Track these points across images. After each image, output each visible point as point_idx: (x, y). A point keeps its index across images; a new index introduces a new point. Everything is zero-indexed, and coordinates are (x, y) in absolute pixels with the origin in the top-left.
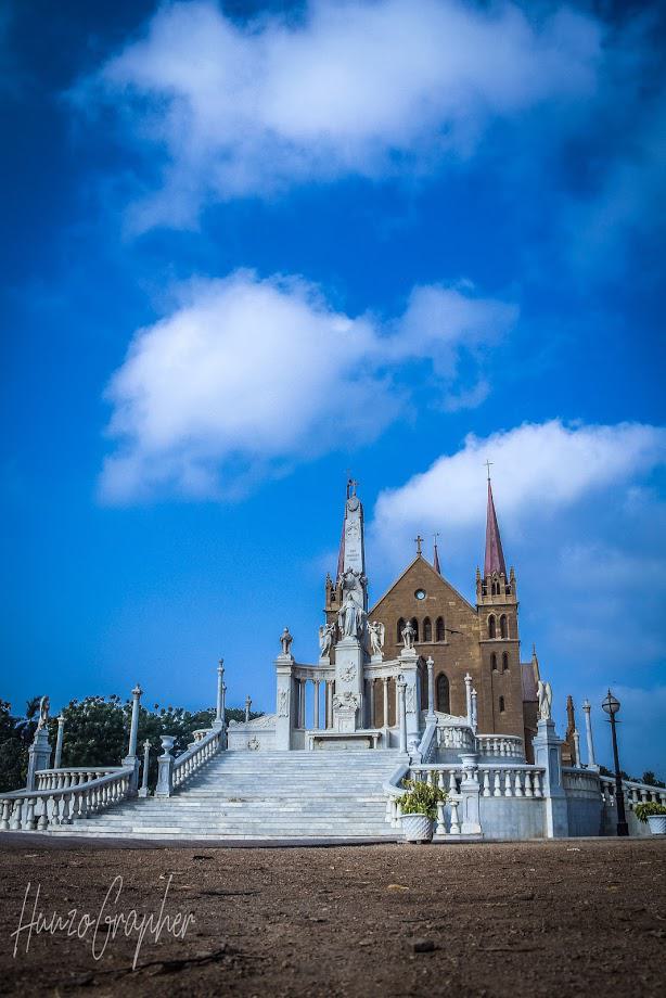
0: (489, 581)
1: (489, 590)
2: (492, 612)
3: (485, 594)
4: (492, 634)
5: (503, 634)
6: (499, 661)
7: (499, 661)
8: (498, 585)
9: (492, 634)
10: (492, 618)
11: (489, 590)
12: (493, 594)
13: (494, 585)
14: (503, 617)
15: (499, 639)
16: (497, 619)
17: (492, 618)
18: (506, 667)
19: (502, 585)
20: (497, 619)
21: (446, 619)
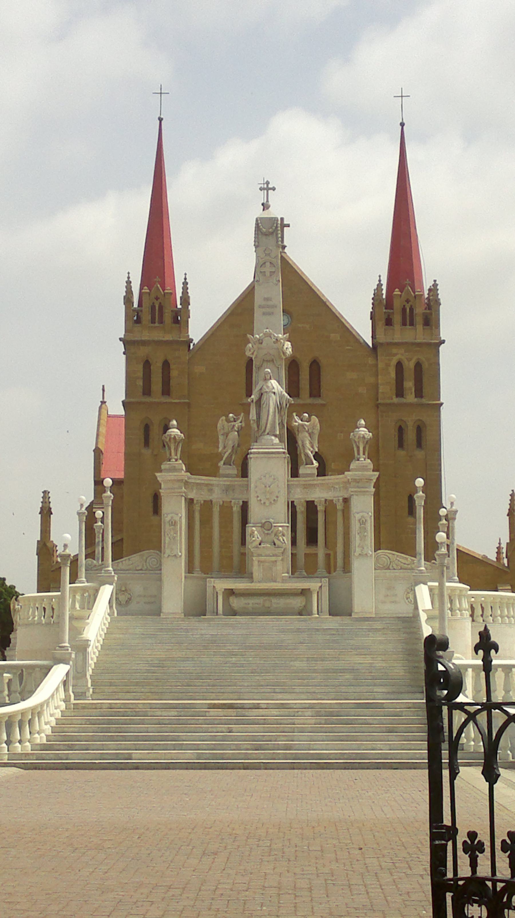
0: (397, 304)
1: (397, 318)
2: (400, 354)
3: (389, 322)
4: (400, 392)
5: (419, 393)
6: (411, 436)
7: (411, 436)
8: (411, 309)
9: (400, 392)
10: (399, 366)
11: (397, 318)
12: (404, 324)
13: (404, 310)
14: (418, 366)
15: (410, 398)
16: (410, 366)
17: (399, 366)
18: (419, 444)
19: (419, 310)
20: (410, 366)
21: (323, 362)
